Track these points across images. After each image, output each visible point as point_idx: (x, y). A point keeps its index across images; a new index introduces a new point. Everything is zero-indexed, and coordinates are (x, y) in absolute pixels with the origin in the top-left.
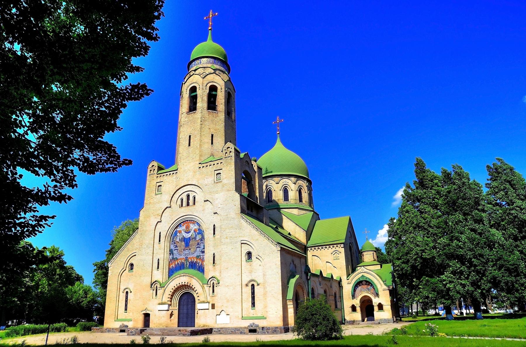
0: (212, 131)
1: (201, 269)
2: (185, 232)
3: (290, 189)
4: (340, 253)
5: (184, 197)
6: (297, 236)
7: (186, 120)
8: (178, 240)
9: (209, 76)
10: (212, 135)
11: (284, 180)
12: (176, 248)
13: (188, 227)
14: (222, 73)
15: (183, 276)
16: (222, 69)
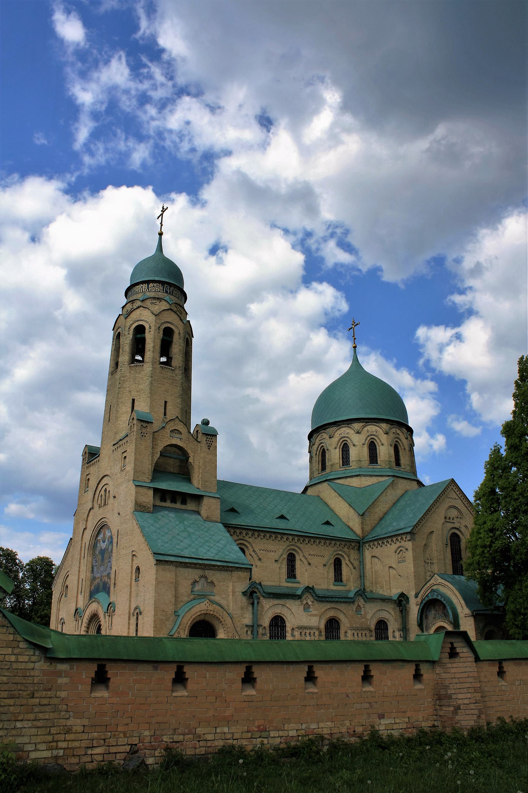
0: (134, 395)
1: (108, 593)
2: (103, 542)
4: (407, 549)
5: (103, 492)
6: (351, 524)
7: (110, 383)
8: (97, 553)
9: (134, 313)
10: (133, 400)
11: (343, 429)
12: (96, 564)
13: (104, 535)
14: (157, 302)
15: (94, 601)
16: (161, 295)
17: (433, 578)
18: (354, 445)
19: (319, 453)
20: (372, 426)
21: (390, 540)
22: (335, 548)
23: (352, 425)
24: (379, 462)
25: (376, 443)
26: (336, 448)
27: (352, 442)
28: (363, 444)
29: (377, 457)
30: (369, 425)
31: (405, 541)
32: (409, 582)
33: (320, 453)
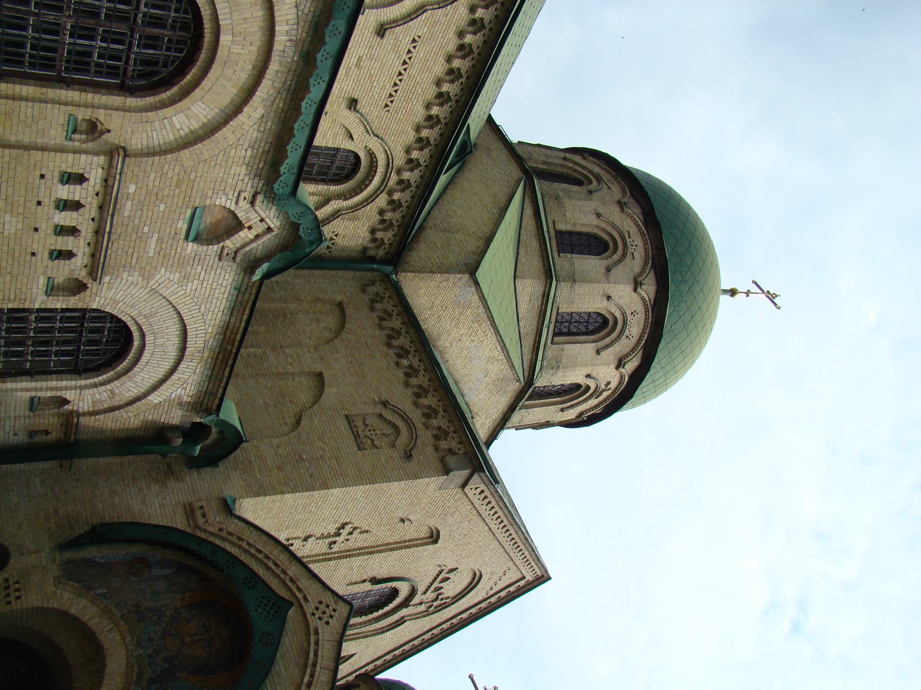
3: (610, 261)
4: (408, 456)
17: (328, 598)
18: (608, 270)
19: (570, 168)
20: (640, 331)
21: (422, 380)
22: (399, 159)
23: (652, 272)
24: (557, 339)
25: (603, 333)
26: (598, 215)
27: (616, 264)
28: (609, 298)
29: (569, 334)
30: (646, 319)
31: (437, 449)
32: (280, 469)
33: (569, 172)
